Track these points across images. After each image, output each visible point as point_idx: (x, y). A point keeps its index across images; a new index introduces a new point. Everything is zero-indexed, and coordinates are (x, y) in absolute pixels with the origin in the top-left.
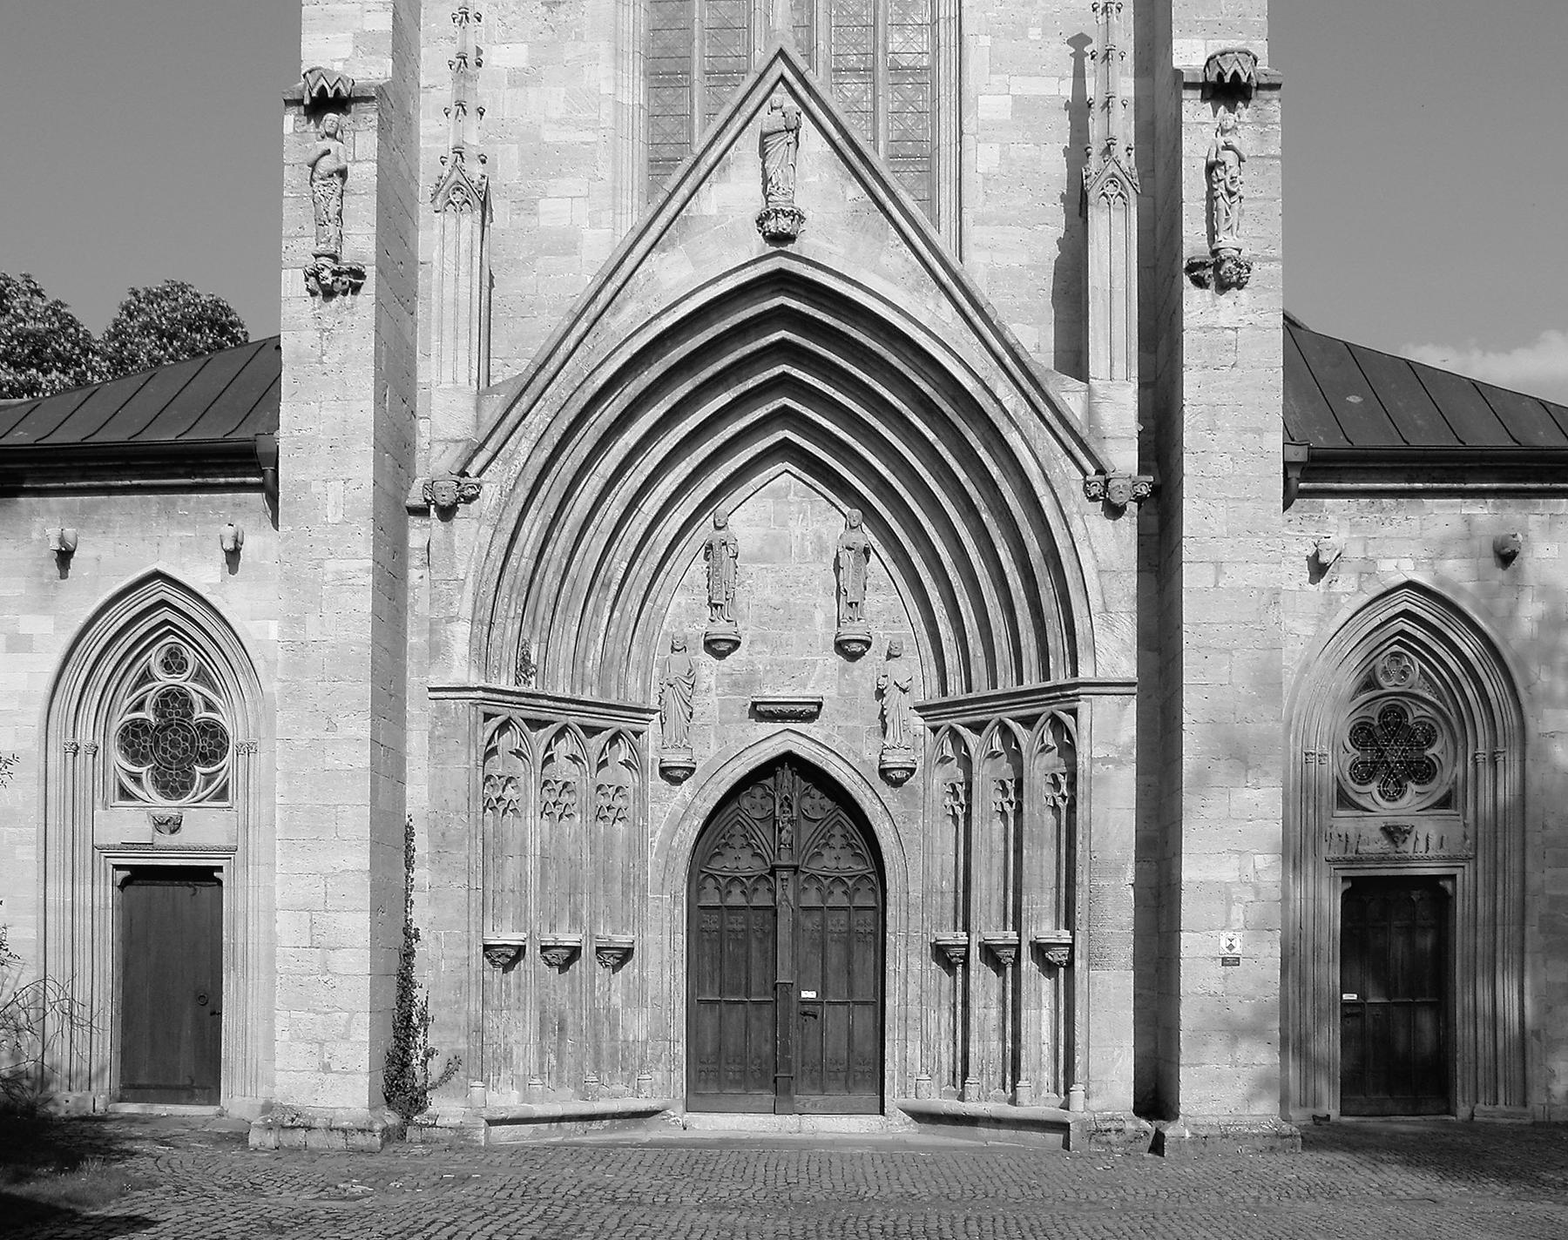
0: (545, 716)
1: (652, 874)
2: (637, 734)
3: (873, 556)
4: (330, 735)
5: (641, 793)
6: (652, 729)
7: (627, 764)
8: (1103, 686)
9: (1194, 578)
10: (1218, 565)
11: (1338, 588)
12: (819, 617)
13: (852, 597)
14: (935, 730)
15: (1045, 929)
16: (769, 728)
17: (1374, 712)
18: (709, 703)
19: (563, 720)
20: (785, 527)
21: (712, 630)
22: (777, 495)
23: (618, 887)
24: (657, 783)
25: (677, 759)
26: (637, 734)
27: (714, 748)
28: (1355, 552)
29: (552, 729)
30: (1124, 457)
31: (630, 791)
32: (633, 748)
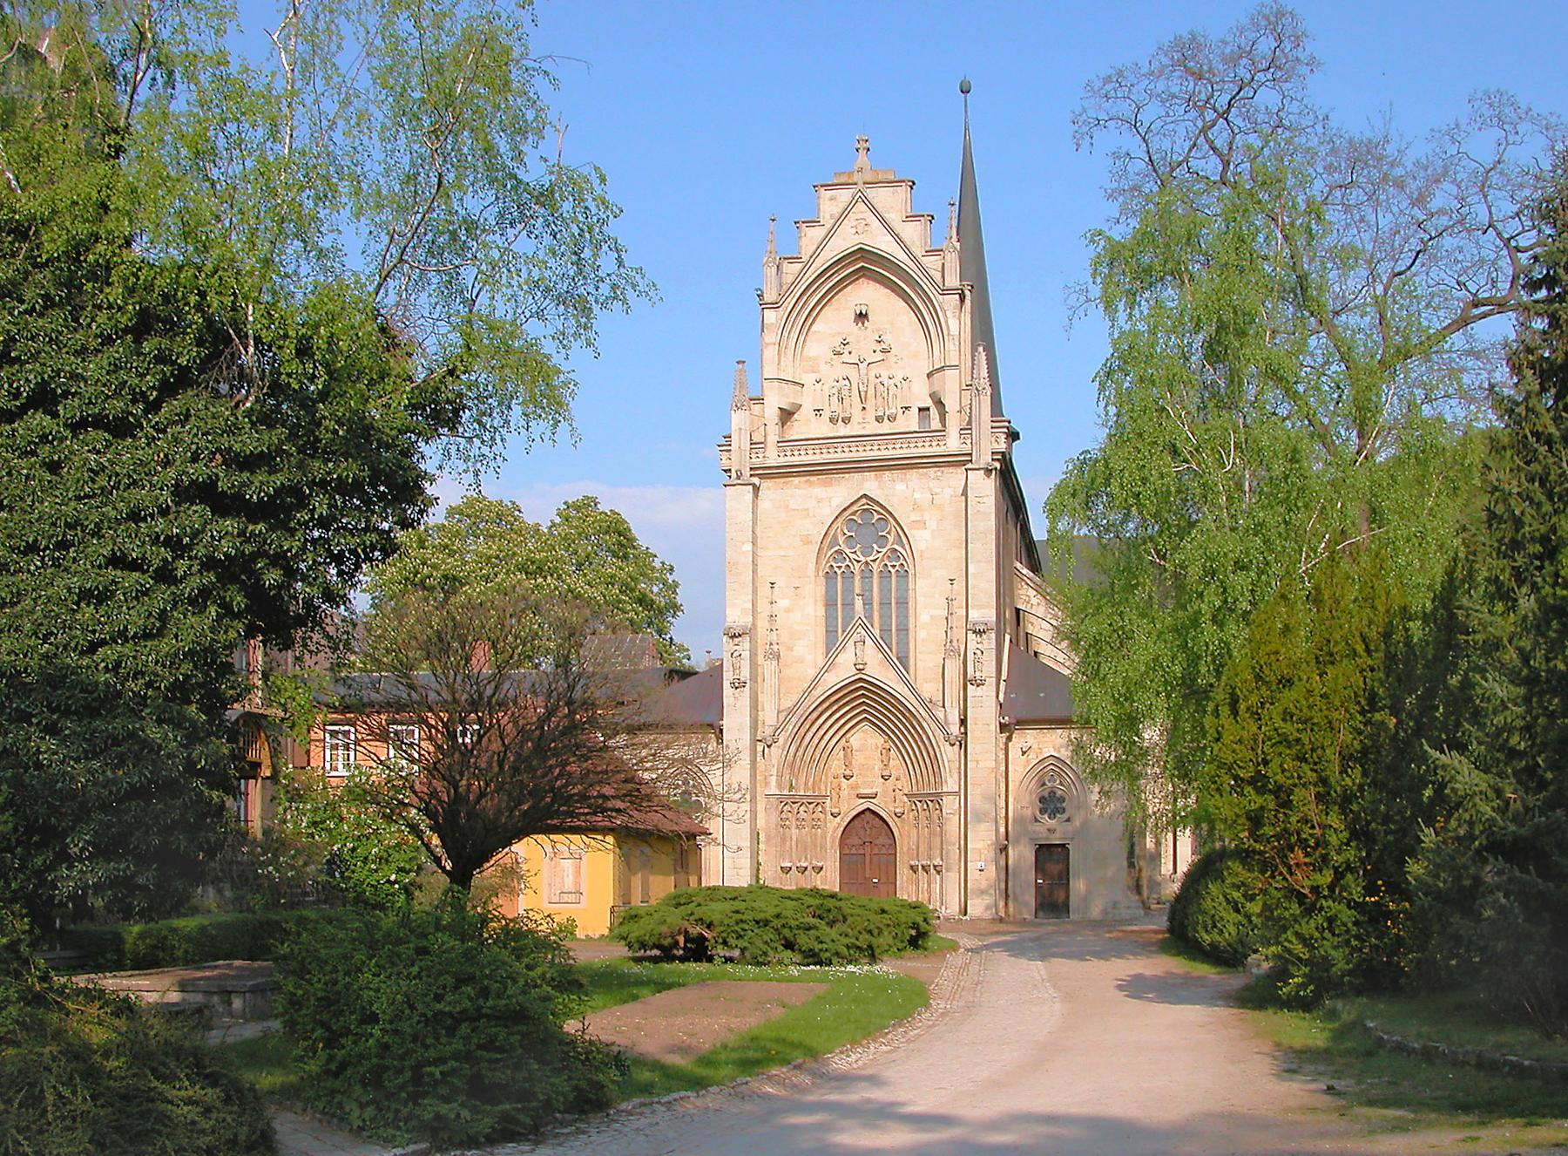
15: (937, 861)
20: (866, 740)
25: (835, 811)
28: (1035, 746)
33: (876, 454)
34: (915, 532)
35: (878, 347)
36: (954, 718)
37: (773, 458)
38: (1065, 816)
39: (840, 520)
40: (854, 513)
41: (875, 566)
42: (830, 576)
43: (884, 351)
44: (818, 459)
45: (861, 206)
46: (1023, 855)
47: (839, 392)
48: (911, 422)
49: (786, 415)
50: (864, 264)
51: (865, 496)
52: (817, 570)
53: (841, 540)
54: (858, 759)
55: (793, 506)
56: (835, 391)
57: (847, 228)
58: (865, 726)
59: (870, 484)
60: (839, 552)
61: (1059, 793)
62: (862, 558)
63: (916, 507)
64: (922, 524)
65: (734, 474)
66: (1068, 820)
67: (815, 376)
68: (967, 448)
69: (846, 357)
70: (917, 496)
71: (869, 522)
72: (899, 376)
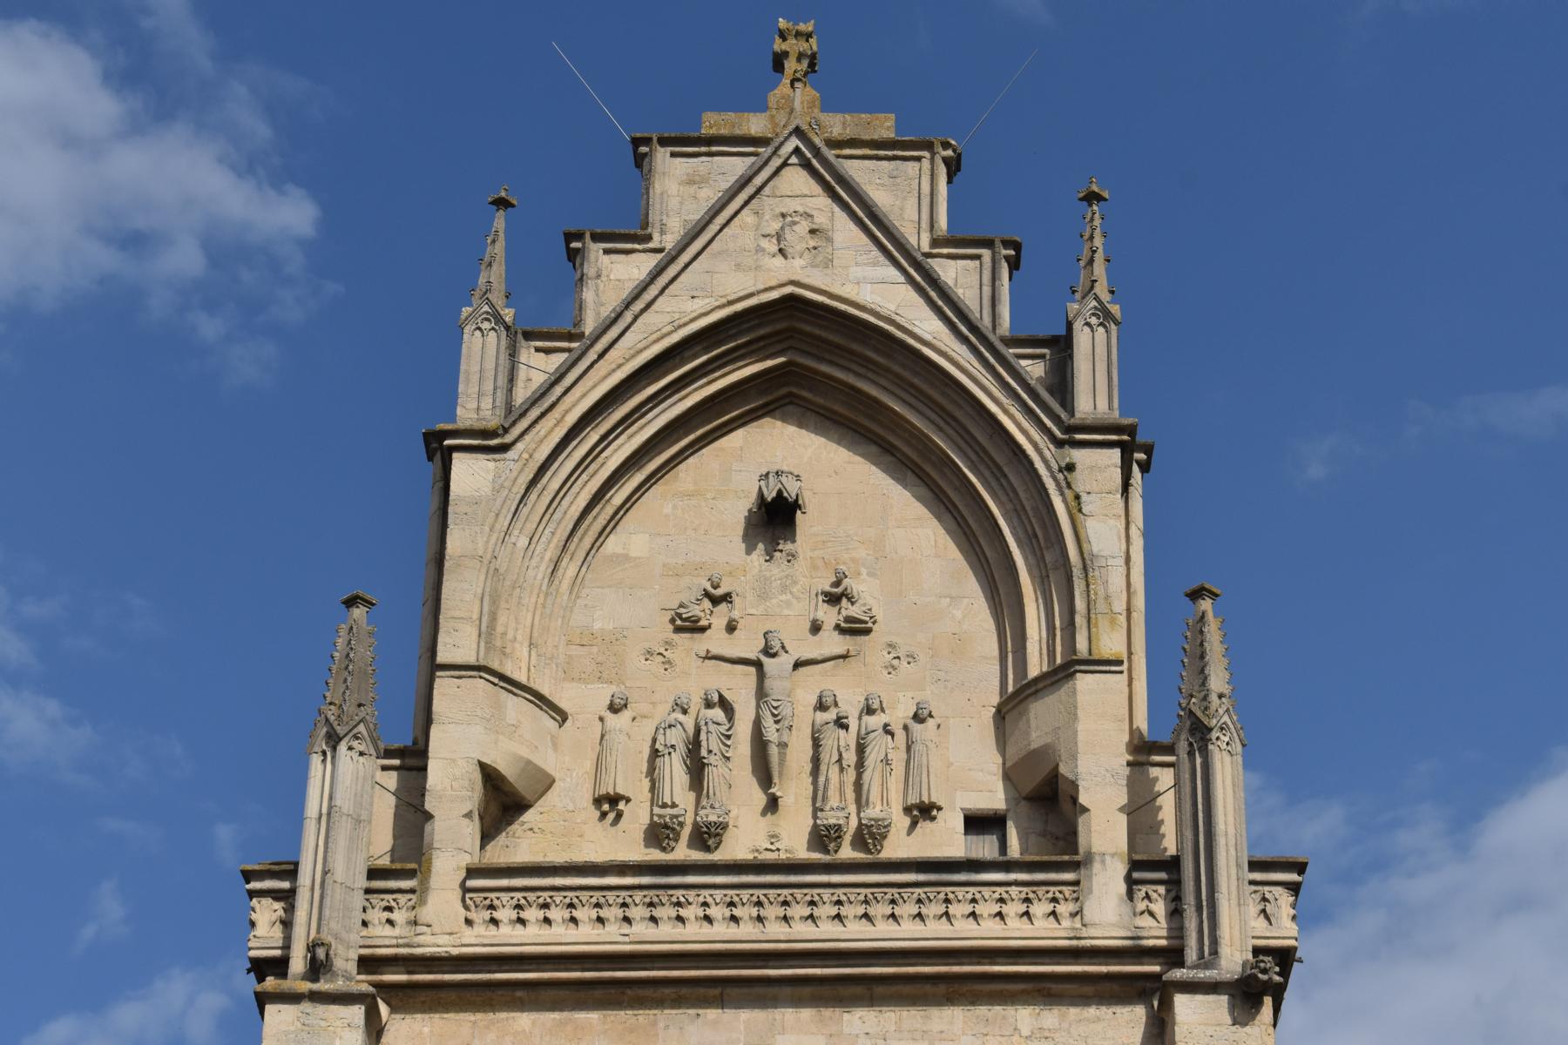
35: (829, 616)
37: (444, 924)
43: (855, 628)
45: (796, 180)
47: (694, 746)
49: (503, 801)
50: (799, 358)
57: (744, 232)
65: (298, 964)
67: (602, 695)
68: (1155, 932)
69: (717, 640)
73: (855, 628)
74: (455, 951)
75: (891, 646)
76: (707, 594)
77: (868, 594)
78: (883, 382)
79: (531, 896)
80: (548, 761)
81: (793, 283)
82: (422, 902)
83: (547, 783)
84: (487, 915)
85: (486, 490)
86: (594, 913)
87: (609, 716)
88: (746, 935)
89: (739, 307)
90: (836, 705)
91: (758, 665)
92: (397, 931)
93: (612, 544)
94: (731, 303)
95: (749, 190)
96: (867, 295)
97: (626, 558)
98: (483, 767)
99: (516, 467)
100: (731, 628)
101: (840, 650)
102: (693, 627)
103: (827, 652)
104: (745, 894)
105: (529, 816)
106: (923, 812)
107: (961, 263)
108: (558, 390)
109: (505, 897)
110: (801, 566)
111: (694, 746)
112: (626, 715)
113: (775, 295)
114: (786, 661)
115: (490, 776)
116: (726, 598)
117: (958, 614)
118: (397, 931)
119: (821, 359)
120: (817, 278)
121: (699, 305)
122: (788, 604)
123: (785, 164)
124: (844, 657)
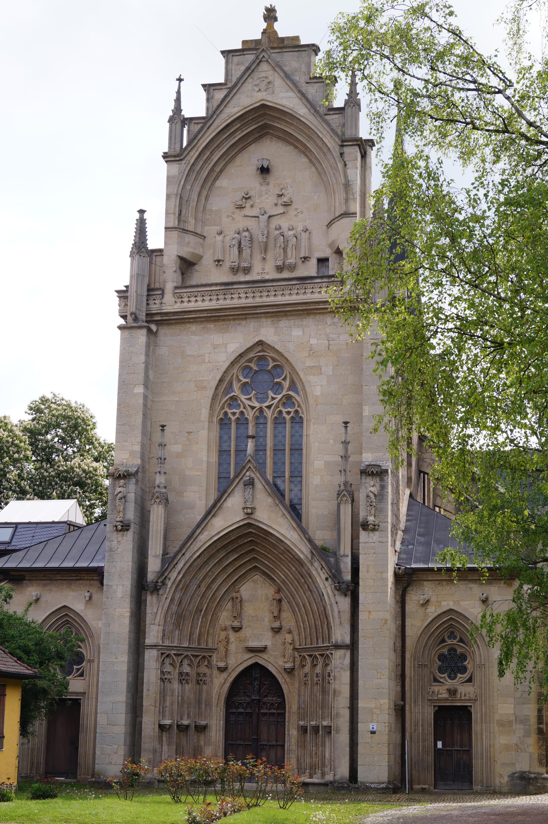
0: (180, 653)
1: (214, 701)
2: (210, 656)
3: (283, 602)
4: (115, 660)
5: (211, 675)
6: (214, 656)
7: (206, 666)
8: (338, 647)
9: (362, 616)
10: (369, 612)
11: (428, 611)
12: (267, 620)
13: (276, 614)
14: (300, 656)
16: (251, 655)
17: (445, 651)
18: (232, 647)
19: (186, 653)
21: (233, 624)
22: (254, 581)
23: (203, 706)
24: (215, 672)
25: (222, 664)
26: (210, 656)
27: (234, 661)
29: (183, 656)
30: (348, 577)
31: (208, 675)
32: (208, 661)
33: (272, 300)
34: (311, 378)
36: (346, 564)
37: (170, 304)
38: (466, 676)
39: (237, 367)
40: (250, 360)
41: (269, 414)
42: (224, 422)
43: (286, 205)
44: (214, 305)
46: (421, 715)
47: (240, 243)
48: (311, 269)
51: (260, 343)
52: (211, 415)
53: (236, 386)
54: (249, 610)
55: (189, 352)
56: (235, 242)
58: (258, 577)
59: (268, 332)
60: (234, 399)
61: (459, 651)
62: (257, 405)
63: (312, 352)
64: (317, 370)
66: (470, 680)
69: (248, 211)
70: (313, 341)
71: (262, 368)
72: (300, 228)
73: (286, 205)
74: (173, 311)
75: (296, 209)
76: (243, 197)
77: (289, 193)
78: (292, 128)
79: (192, 294)
80: (199, 251)
81: (263, 100)
82: (163, 297)
83: (201, 257)
84: (180, 300)
85: (177, 174)
86: (209, 298)
87: (217, 236)
88: (250, 302)
89: (248, 109)
90: (280, 228)
91: (258, 217)
92: (157, 306)
93: (218, 183)
94: (245, 108)
95: (250, 71)
96: (285, 102)
97: (221, 187)
98: (179, 256)
99: (185, 166)
100: (252, 206)
101: (282, 211)
102: (241, 207)
103: (278, 212)
104: (250, 290)
105: (196, 267)
106: (306, 259)
107: (318, 84)
108: (196, 141)
109: (185, 294)
110: (271, 186)
111: (240, 243)
112: (223, 235)
113: (258, 104)
114: (266, 216)
115: (182, 259)
116: (249, 198)
117: (316, 198)
118: (157, 306)
119: (274, 122)
120: (270, 98)
121: (236, 109)
122: (268, 198)
123: (261, 61)
124: (284, 213)
